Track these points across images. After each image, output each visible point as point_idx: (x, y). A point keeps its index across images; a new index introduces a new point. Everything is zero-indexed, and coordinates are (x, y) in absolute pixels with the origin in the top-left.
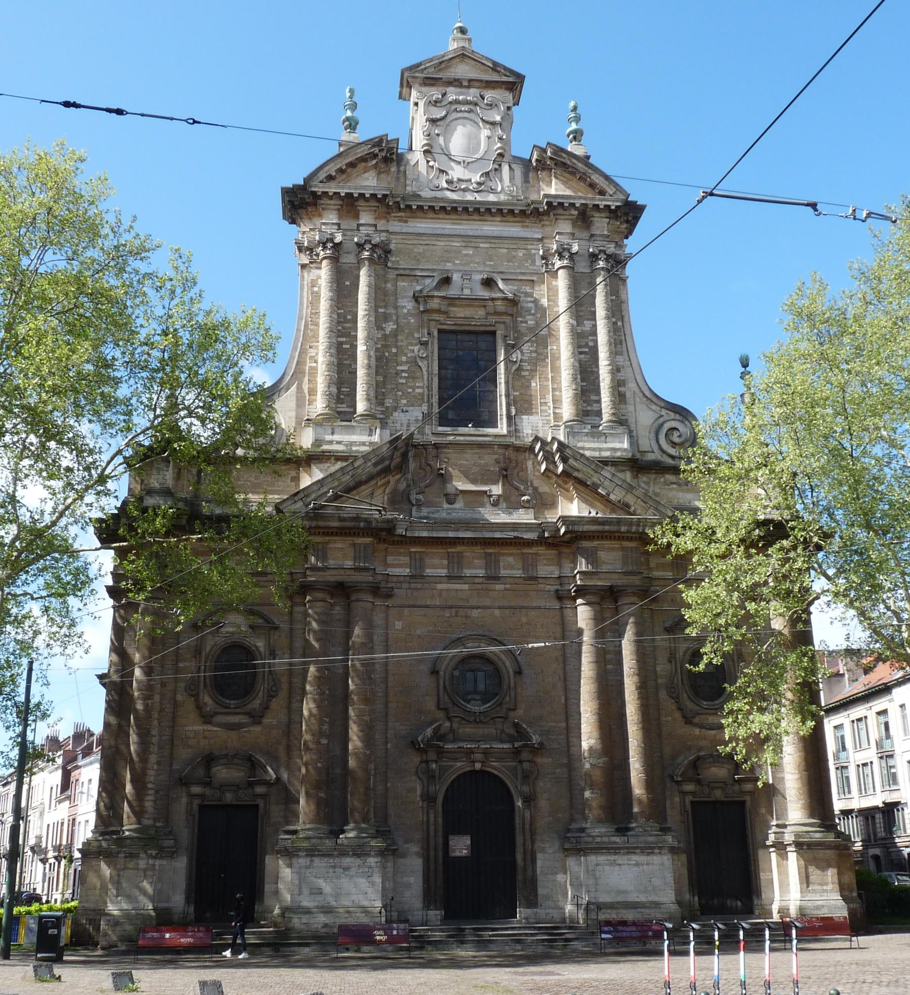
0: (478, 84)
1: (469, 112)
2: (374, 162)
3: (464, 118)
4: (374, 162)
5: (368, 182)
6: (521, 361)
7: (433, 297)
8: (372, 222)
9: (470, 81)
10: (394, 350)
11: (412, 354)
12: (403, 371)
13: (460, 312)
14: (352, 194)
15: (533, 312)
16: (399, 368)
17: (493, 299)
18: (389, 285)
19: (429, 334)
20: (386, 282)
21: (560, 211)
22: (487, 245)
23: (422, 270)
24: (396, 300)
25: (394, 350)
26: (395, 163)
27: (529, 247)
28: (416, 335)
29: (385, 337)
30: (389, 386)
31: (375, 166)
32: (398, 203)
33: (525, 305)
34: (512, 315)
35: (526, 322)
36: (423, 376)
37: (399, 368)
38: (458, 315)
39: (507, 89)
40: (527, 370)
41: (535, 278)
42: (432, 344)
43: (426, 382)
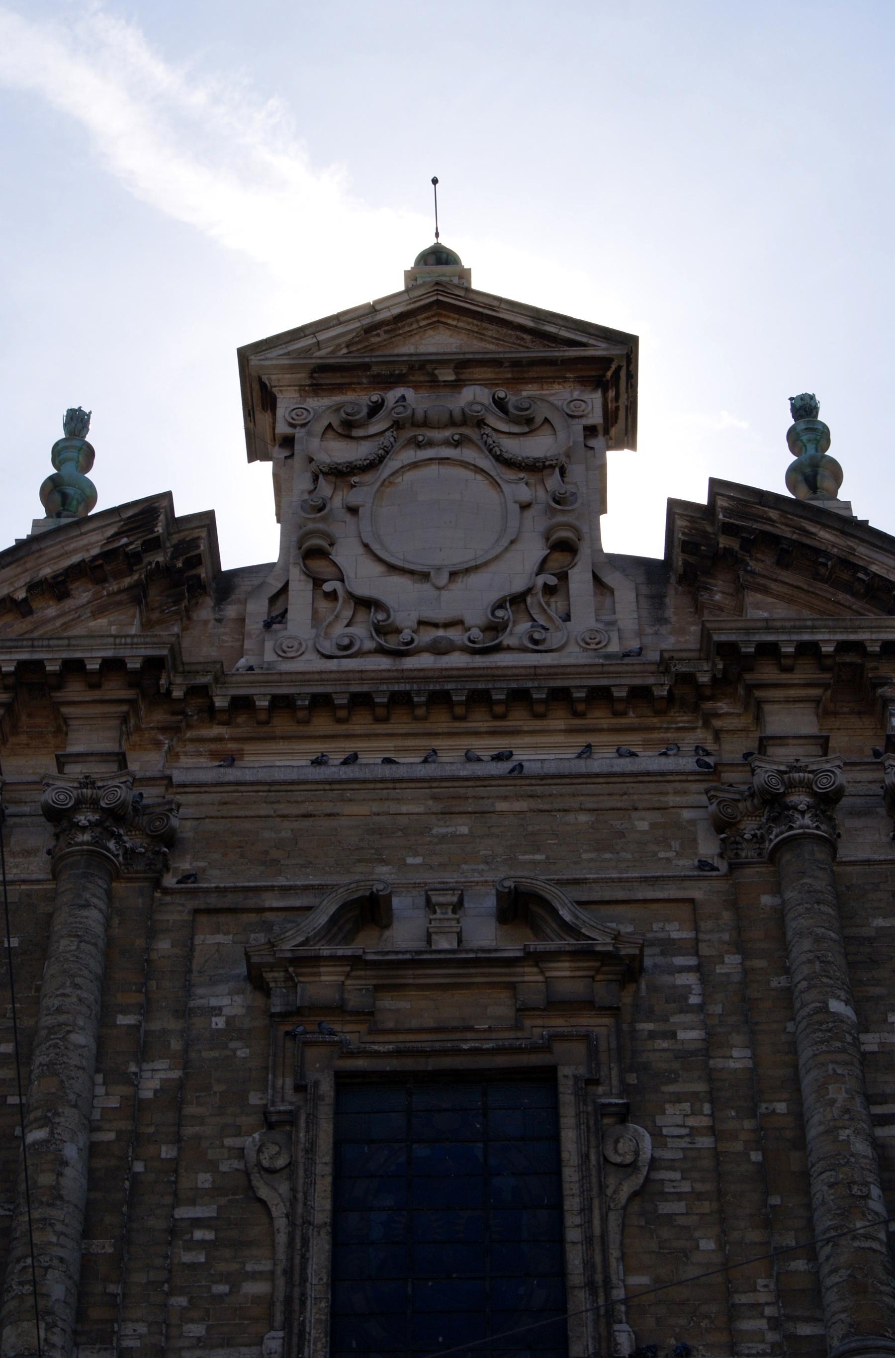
0: (488, 373)
1: (457, 444)
2: (127, 581)
3: (443, 461)
4: (127, 581)
5: (102, 630)
6: (654, 1163)
7: (316, 960)
8: (110, 746)
9: (462, 364)
10: (167, 1152)
11: (236, 1164)
12: (197, 1223)
13: (413, 1010)
14: (39, 665)
15: (694, 1000)
16: (183, 1212)
17: (536, 958)
18: (164, 945)
19: (300, 1088)
20: (152, 933)
21: (768, 673)
22: (521, 805)
23: (285, 890)
24: (188, 988)
25: (167, 1152)
26: (209, 602)
27: (672, 800)
28: (255, 1099)
29: (136, 1107)
30: (139, 1278)
31: (137, 595)
32: (202, 691)
33: (666, 979)
34: (614, 1011)
35: (673, 1035)
36: (272, 1232)
37: (183, 1212)
38: (414, 1023)
39: (584, 382)
40: (680, 1196)
41: (698, 892)
42: (312, 1120)
43: (281, 1254)
